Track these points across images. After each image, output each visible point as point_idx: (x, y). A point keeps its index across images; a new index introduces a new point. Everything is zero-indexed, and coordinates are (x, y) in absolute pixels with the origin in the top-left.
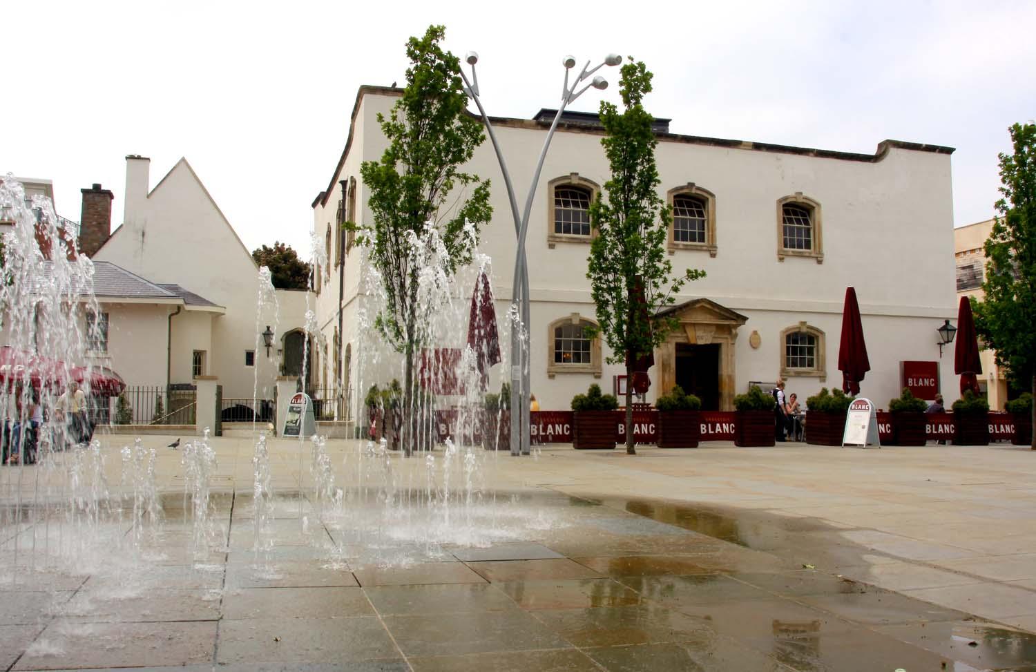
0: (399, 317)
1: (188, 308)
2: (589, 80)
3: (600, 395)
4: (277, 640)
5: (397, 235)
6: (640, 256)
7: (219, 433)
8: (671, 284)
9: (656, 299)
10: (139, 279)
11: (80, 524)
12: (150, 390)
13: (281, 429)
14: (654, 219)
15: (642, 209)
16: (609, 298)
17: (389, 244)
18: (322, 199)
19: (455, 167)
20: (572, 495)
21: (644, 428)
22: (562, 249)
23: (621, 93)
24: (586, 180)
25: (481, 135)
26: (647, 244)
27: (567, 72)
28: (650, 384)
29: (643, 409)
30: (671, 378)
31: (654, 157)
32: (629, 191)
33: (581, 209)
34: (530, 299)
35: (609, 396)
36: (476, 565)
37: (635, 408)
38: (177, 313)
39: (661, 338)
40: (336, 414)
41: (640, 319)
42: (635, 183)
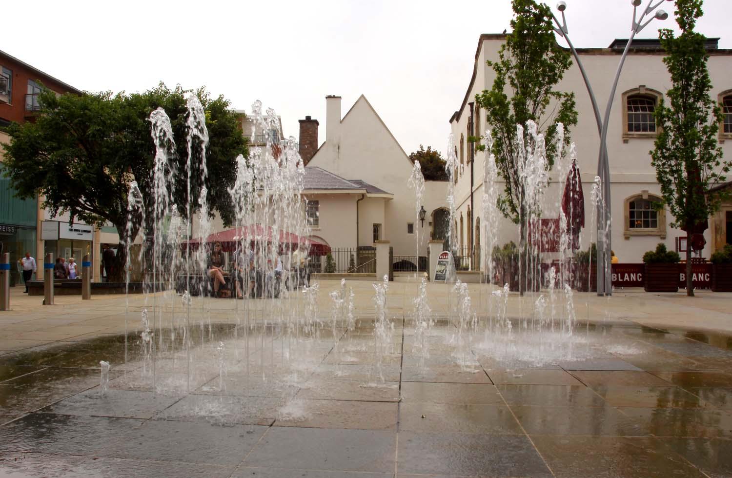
0: (514, 197)
1: (369, 195)
2: (653, 13)
3: (665, 252)
4: (423, 417)
5: (510, 139)
6: (696, 145)
7: (391, 279)
8: (722, 165)
9: (710, 178)
10: (337, 177)
11: (284, 339)
12: (346, 250)
13: (433, 276)
14: (708, 116)
15: (698, 109)
16: (672, 178)
17: (504, 146)
18: (457, 116)
19: (551, 87)
20: (645, 325)
21: (701, 277)
22: (634, 144)
23: (677, 20)
24: (652, 90)
25: (569, 61)
26: (702, 136)
27: (635, 9)
28: (705, 243)
29: (700, 262)
30: (722, 238)
31: (707, 69)
32: (687, 96)
33: (648, 112)
34: (611, 181)
35: (672, 252)
36: (573, 373)
37: (693, 262)
38: (362, 199)
39: (715, 208)
40: (470, 266)
41: (697, 193)
42: (691, 89)
